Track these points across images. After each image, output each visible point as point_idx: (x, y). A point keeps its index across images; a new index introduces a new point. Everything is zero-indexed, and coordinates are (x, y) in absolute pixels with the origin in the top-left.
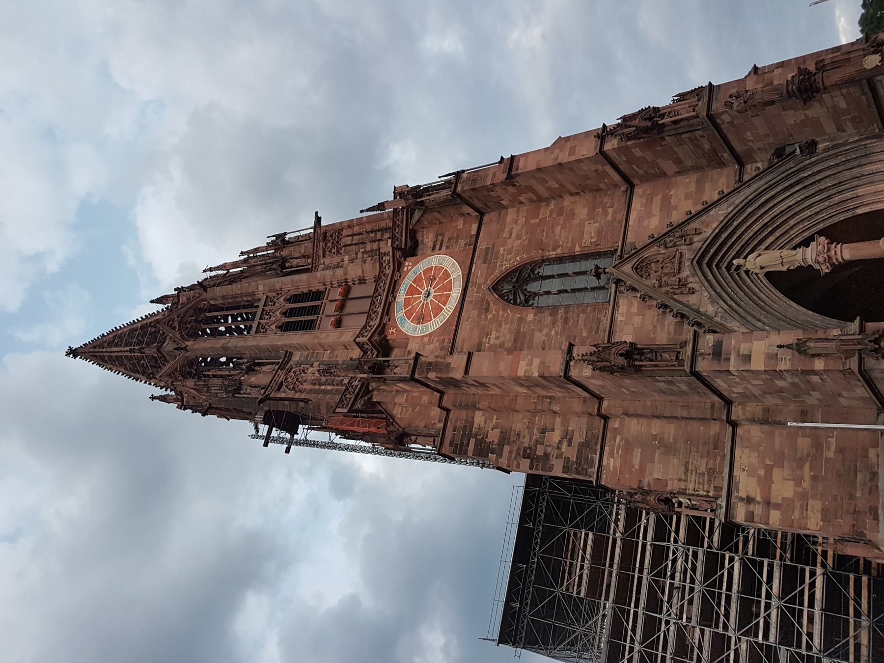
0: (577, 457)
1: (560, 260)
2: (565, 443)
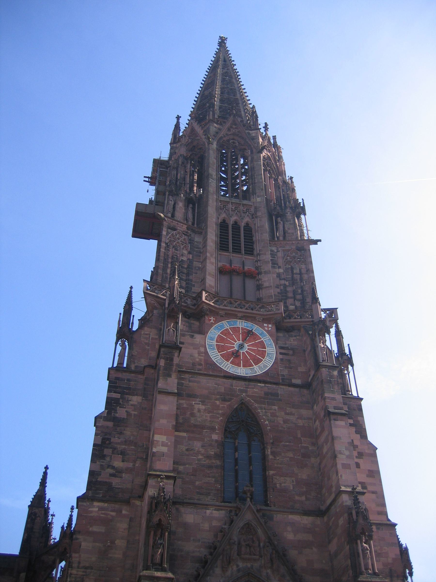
0: (100, 482)
1: (264, 458)
2: (111, 471)
